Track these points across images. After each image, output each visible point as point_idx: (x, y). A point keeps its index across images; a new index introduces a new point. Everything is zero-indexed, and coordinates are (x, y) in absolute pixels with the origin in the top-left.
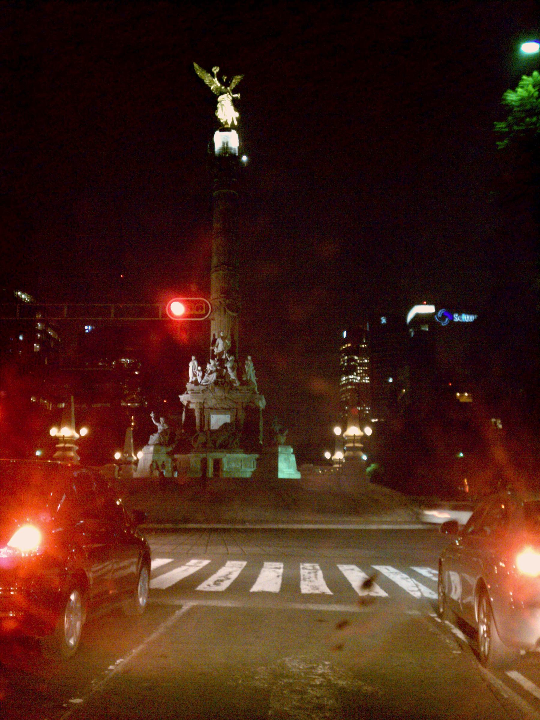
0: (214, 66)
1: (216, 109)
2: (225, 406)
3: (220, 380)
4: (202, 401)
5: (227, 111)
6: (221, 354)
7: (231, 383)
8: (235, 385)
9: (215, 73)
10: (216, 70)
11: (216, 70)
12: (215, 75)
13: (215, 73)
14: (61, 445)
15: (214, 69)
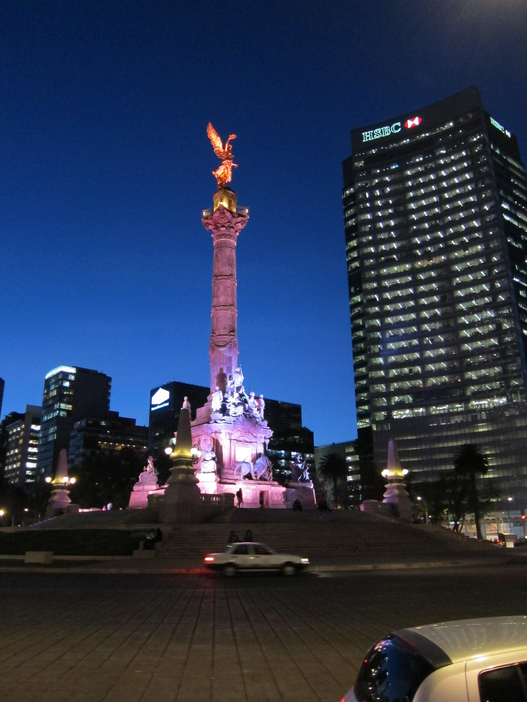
0: (235, 134)
1: (216, 168)
2: (247, 440)
3: (247, 413)
4: (230, 432)
5: (224, 172)
6: (238, 389)
7: (254, 417)
8: (258, 420)
9: (229, 139)
10: (232, 137)
11: (232, 137)
12: (228, 141)
13: (229, 139)
14: (184, 467)
15: (233, 135)
